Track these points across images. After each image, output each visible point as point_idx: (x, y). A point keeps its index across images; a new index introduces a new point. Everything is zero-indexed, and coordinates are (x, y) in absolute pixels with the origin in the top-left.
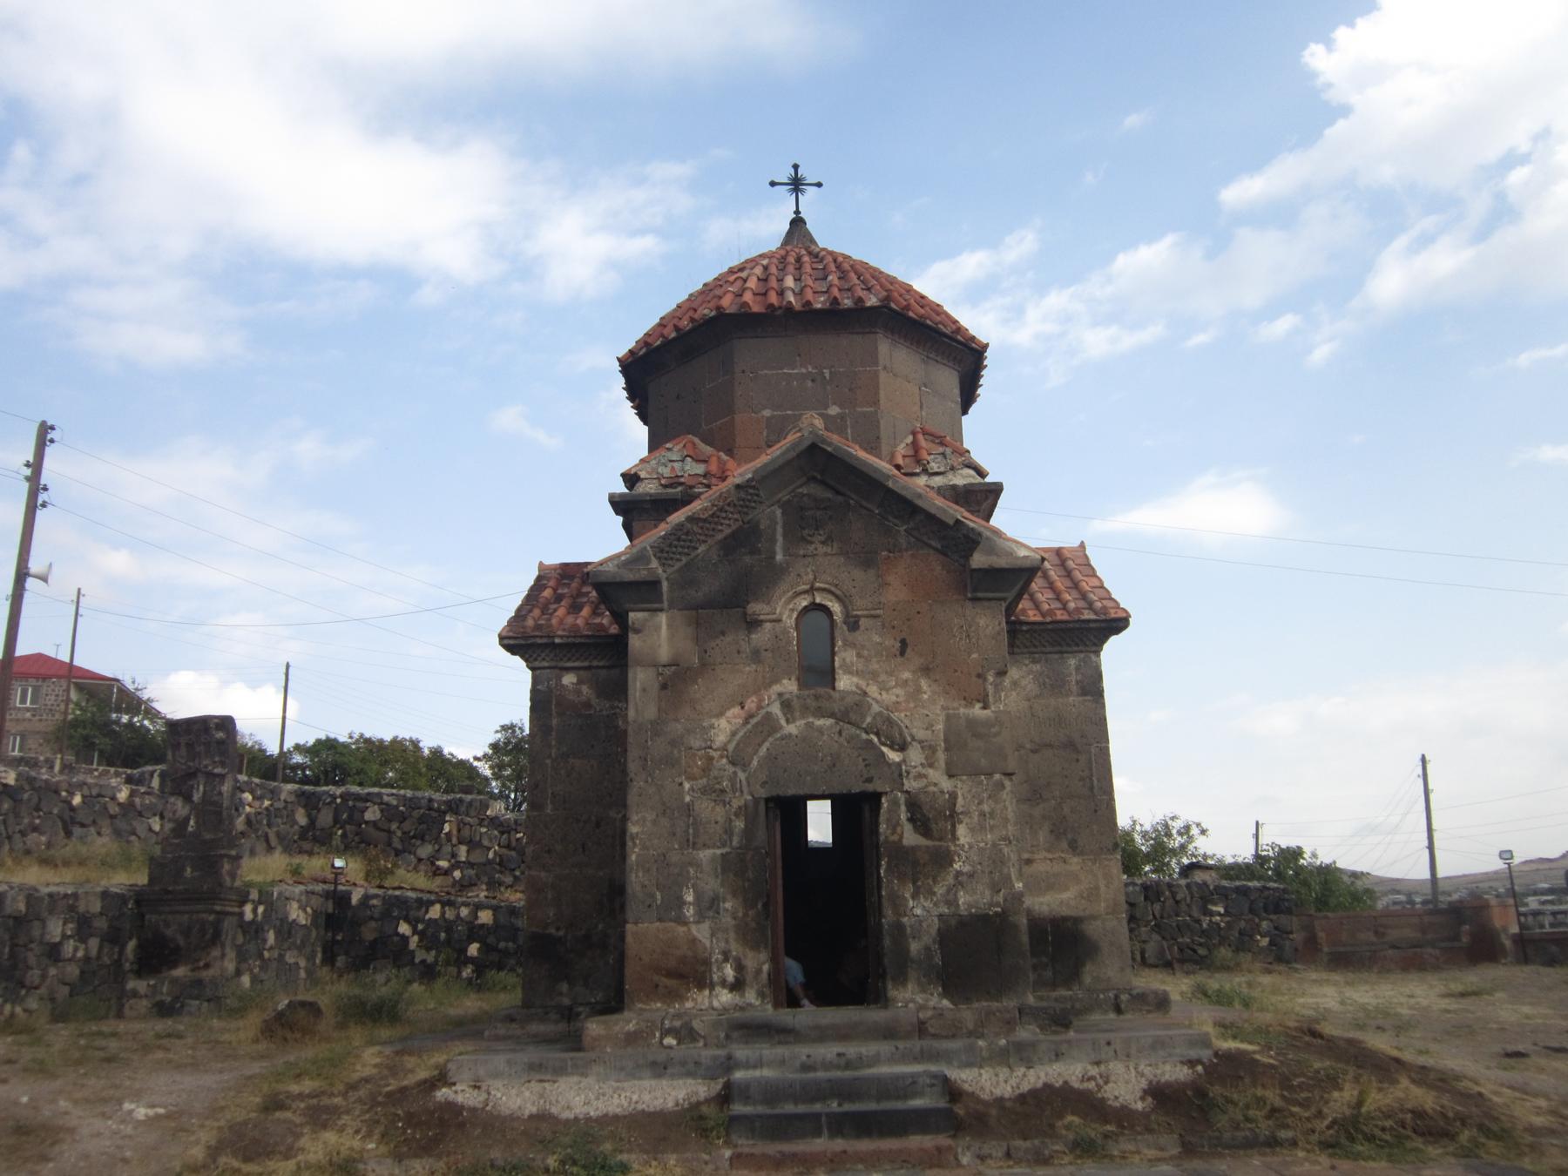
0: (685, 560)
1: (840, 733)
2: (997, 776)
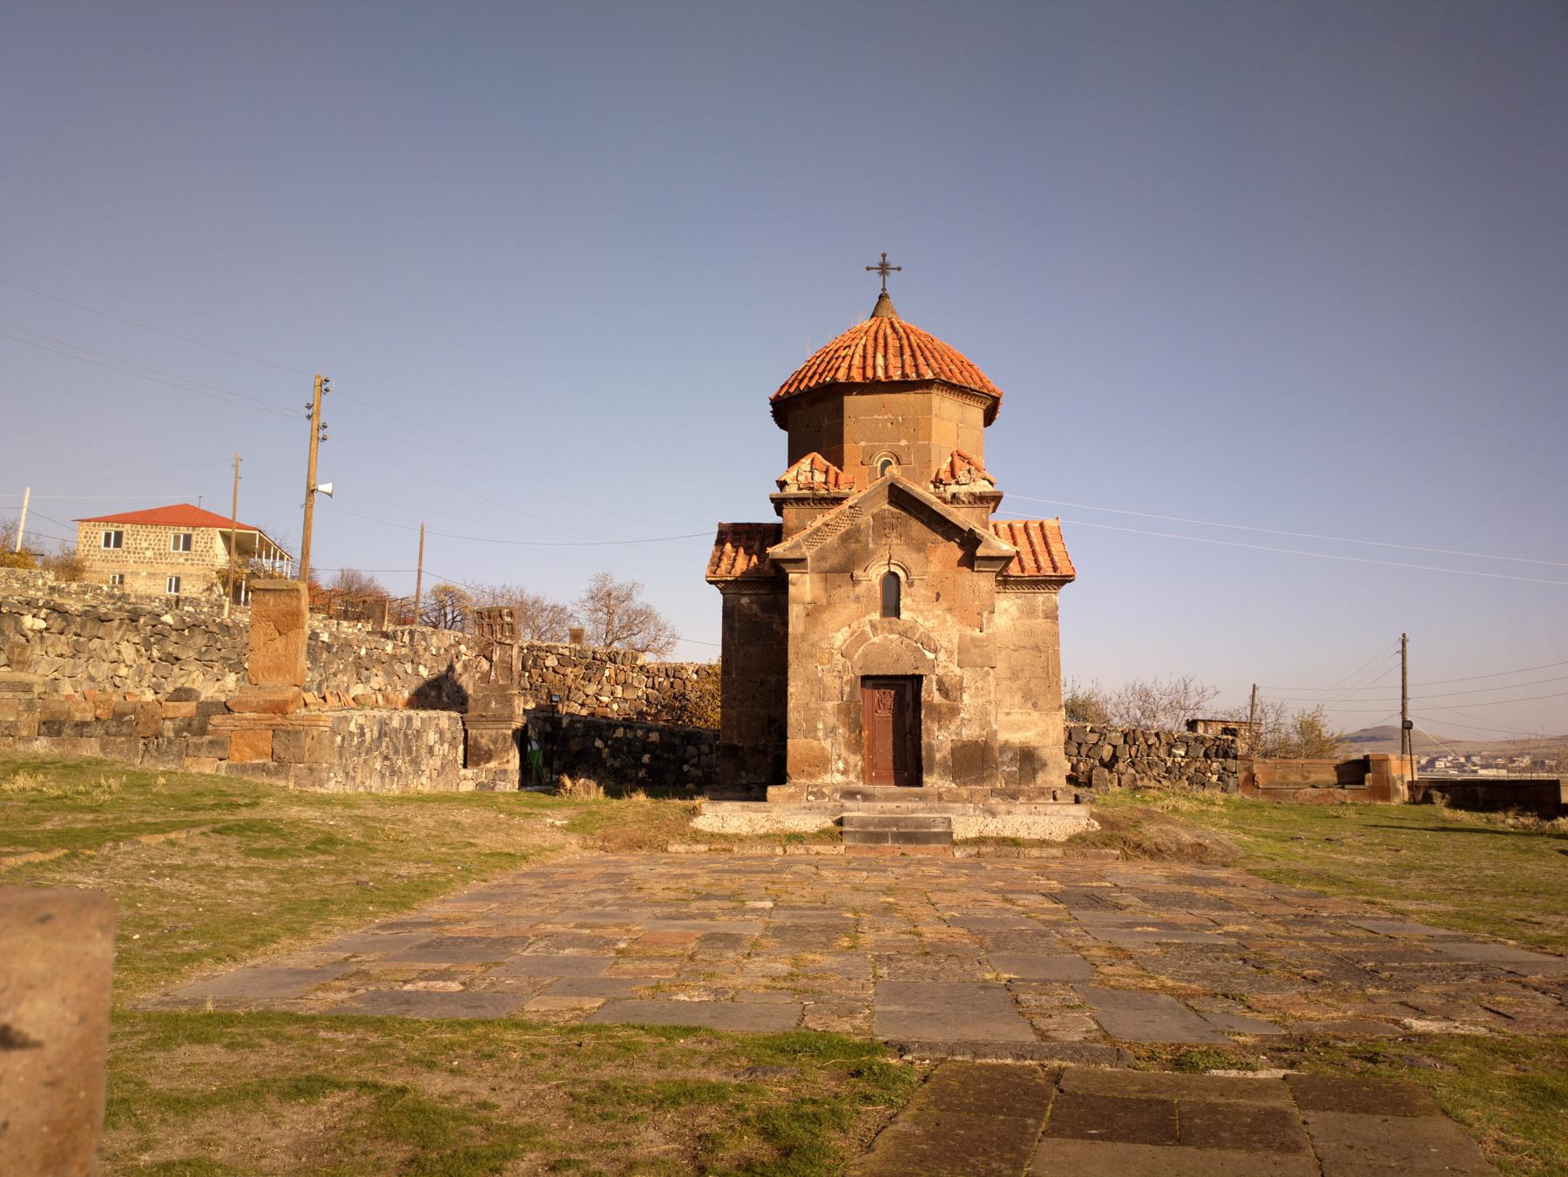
2: (986, 668)
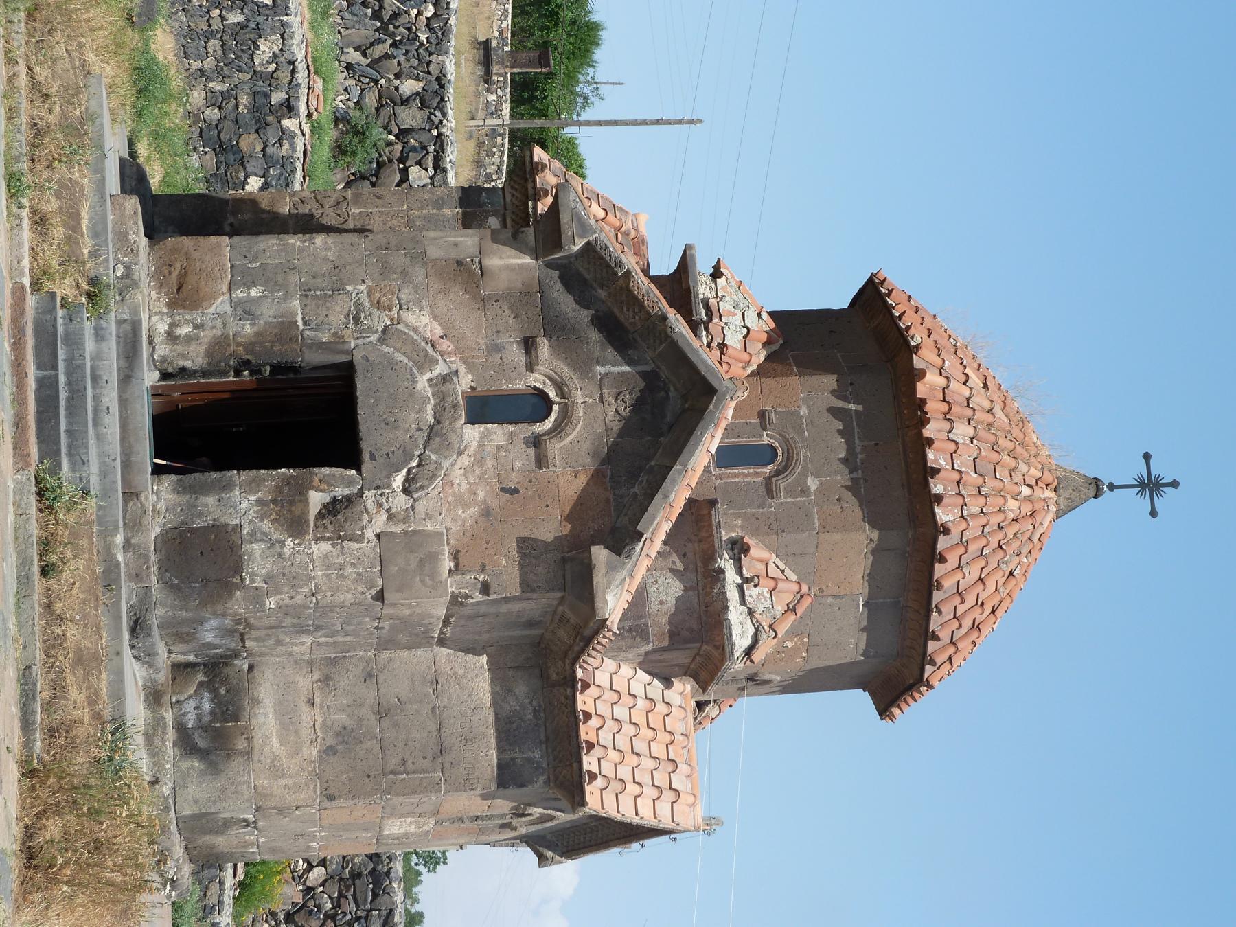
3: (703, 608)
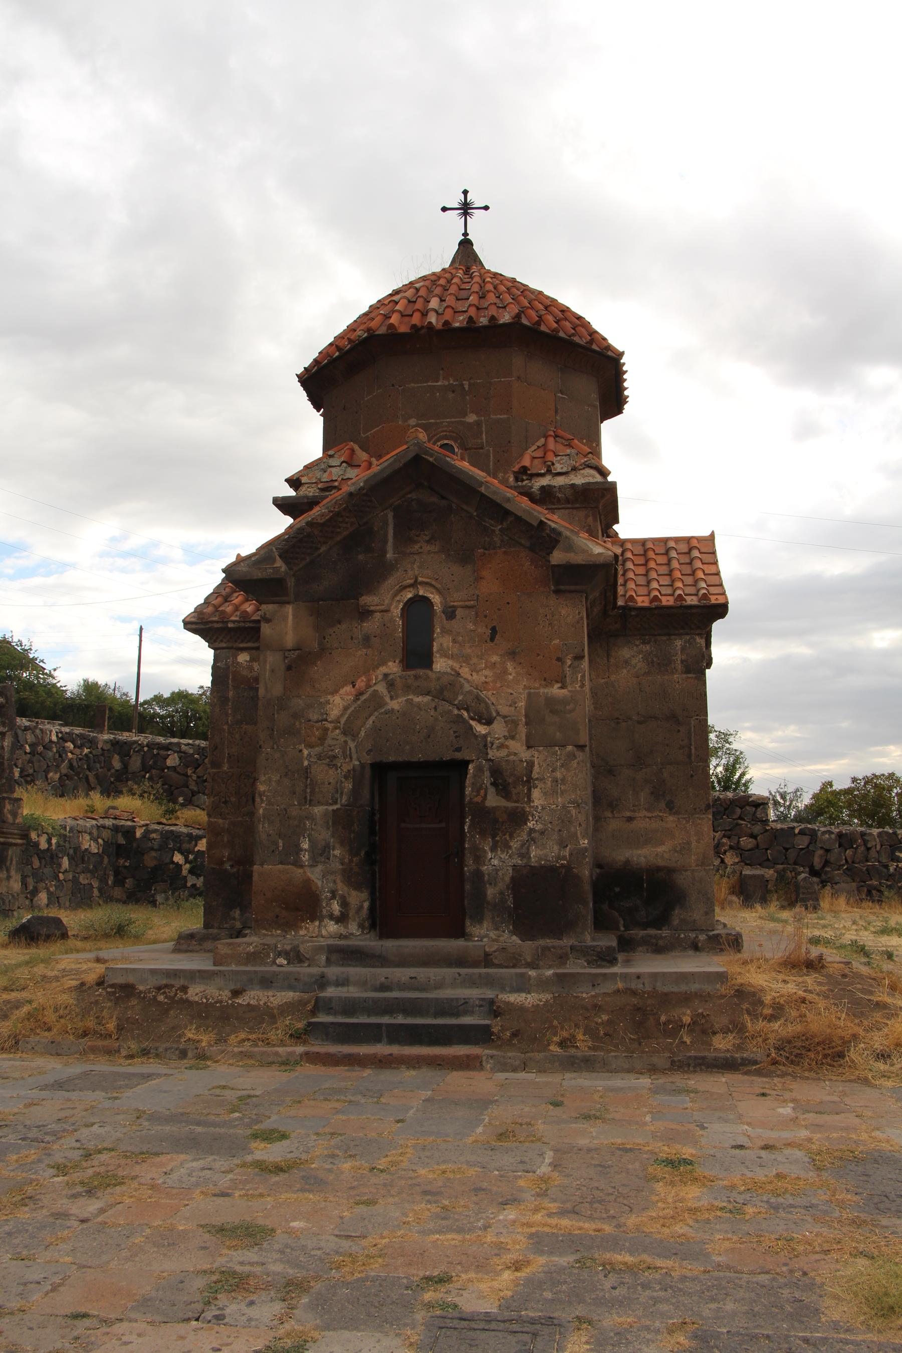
0: (308, 560)
1: (435, 708)
2: (570, 748)
3: (569, 506)
